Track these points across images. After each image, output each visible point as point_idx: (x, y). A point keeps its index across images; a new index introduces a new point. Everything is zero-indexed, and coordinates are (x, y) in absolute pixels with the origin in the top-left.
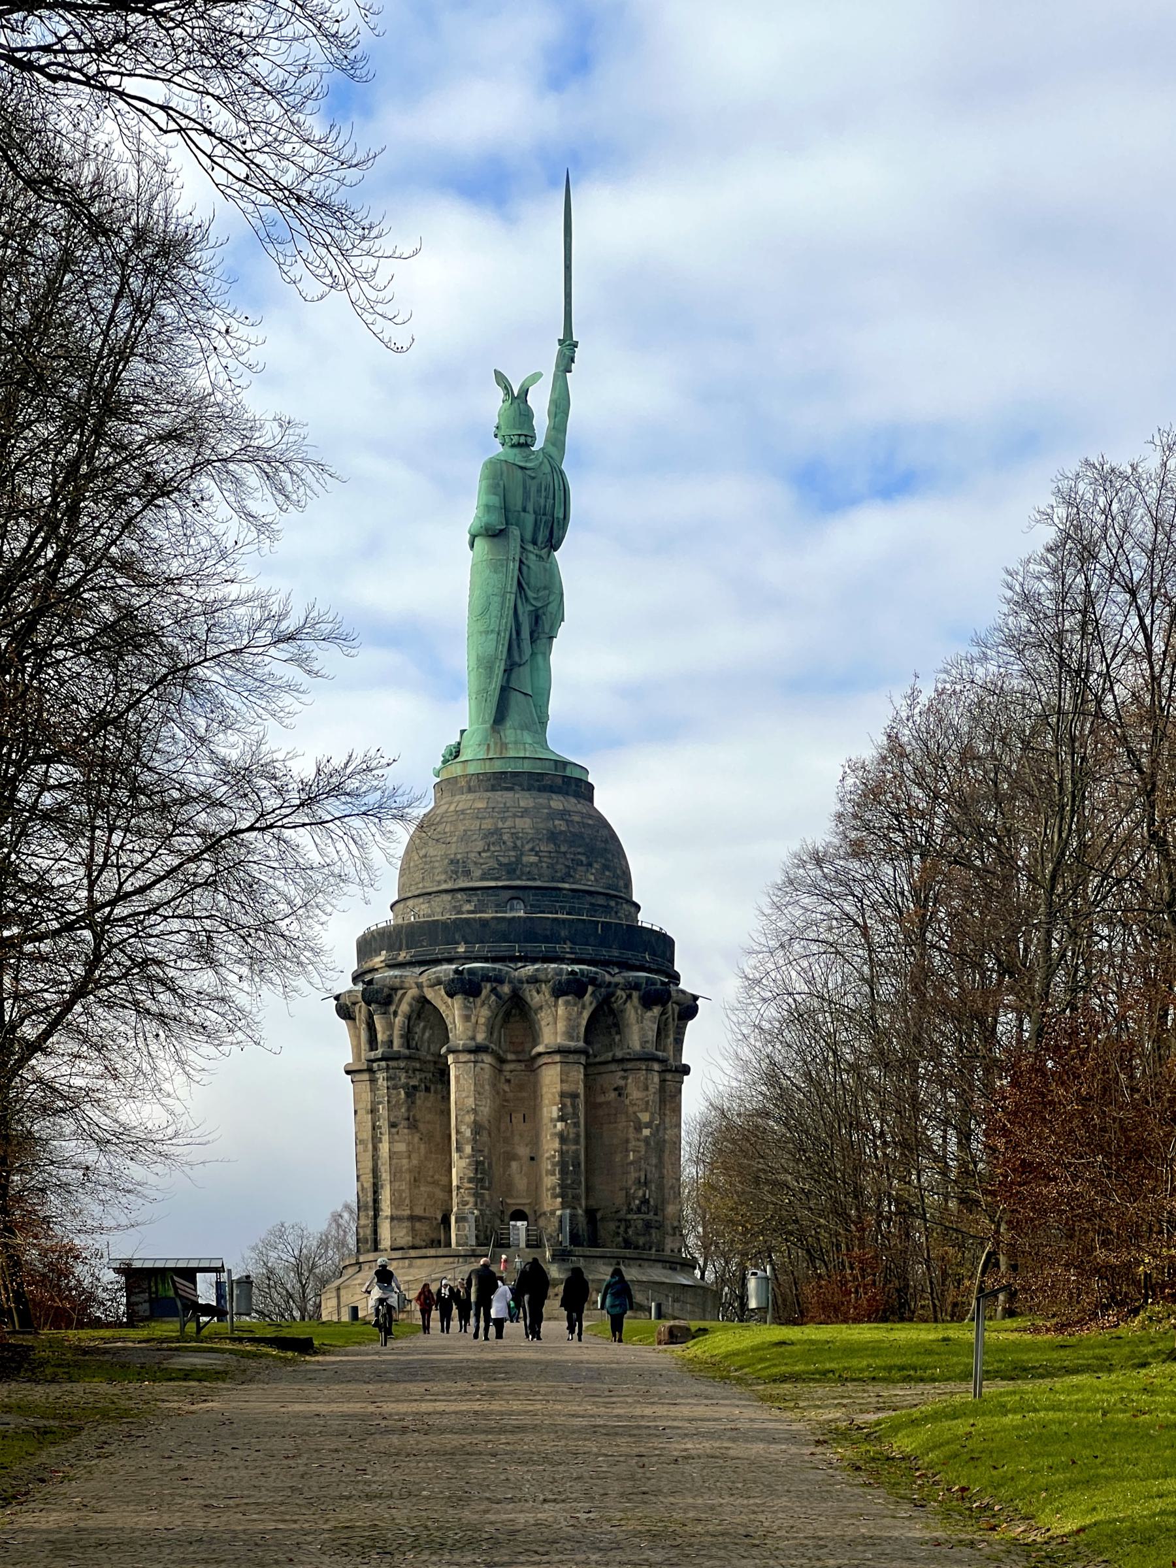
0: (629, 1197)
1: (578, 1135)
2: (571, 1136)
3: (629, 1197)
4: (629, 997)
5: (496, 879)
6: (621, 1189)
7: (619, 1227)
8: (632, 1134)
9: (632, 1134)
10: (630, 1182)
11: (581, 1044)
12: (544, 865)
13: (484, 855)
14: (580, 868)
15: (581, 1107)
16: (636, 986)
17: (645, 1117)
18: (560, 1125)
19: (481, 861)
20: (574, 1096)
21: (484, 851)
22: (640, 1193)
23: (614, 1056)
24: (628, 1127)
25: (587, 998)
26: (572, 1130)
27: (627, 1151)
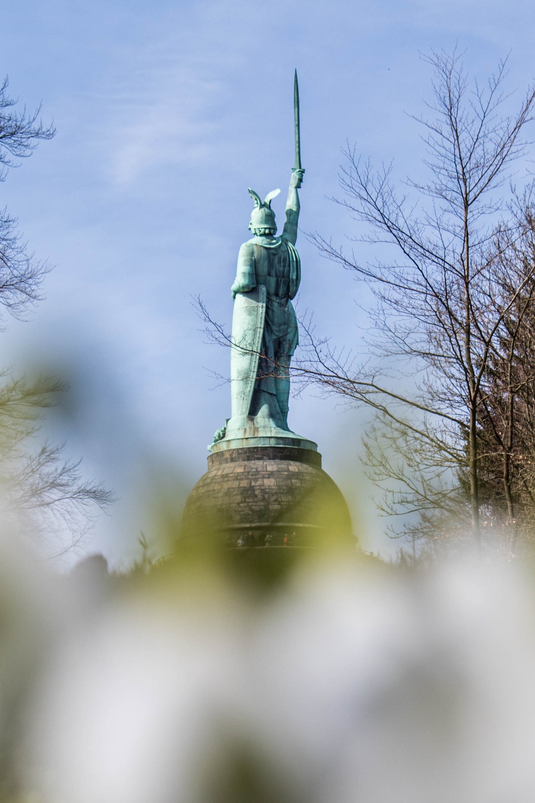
19: (240, 509)
21: (242, 502)
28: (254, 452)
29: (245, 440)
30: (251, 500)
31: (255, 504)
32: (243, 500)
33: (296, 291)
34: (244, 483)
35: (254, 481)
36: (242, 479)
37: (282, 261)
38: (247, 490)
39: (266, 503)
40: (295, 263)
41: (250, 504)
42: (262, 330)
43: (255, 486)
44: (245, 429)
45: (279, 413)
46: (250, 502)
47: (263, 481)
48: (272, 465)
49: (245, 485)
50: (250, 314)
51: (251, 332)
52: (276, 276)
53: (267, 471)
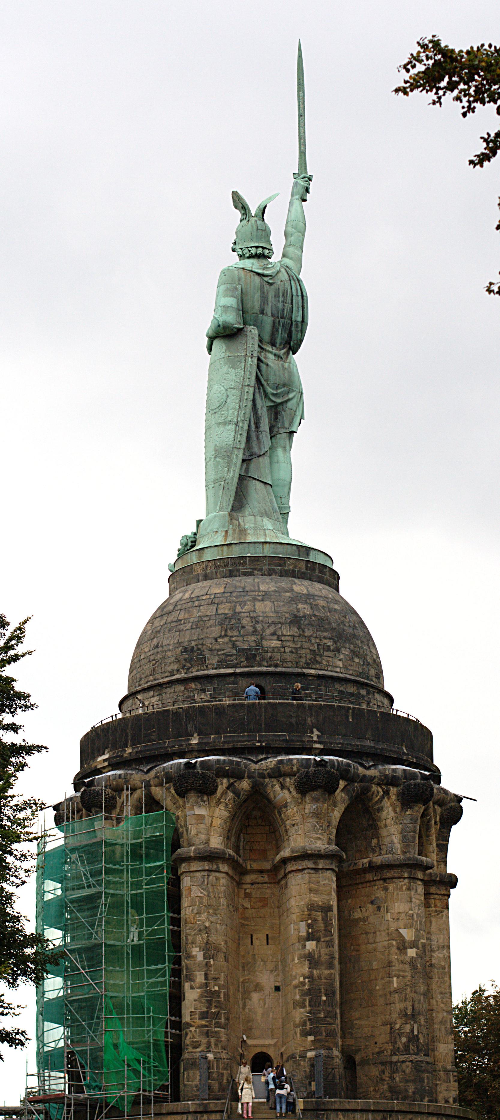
0: (394, 1035)
1: (332, 957)
2: (324, 958)
3: (394, 1035)
4: (386, 793)
5: (235, 666)
6: (384, 1024)
7: (383, 1072)
8: (394, 957)
9: (395, 956)
10: (395, 1016)
11: (334, 847)
12: (287, 650)
13: (220, 640)
14: (326, 653)
15: (335, 922)
16: (392, 781)
17: (408, 934)
18: (311, 945)
19: (218, 647)
20: (327, 909)
21: (221, 637)
22: (407, 1028)
23: (370, 863)
24: (390, 946)
25: (339, 794)
26: (324, 951)
27: (390, 976)
28: (240, 564)
29: (225, 548)
30: (236, 633)
31: (241, 639)
32: (223, 633)
33: (301, 341)
34: (225, 609)
35: (240, 605)
36: (222, 603)
37: (281, 294)
38: (230, 619)
39: (259, 637)
40: (300, 298)
41: (234, 639)
42: (251, 390)
43: (241, 612)
44: (226, 532)
45: (276, 512)
46: (233, 637)
47: (254, 605)
48: (267, 583)
49: (227, 611)
50: (233, 367)
51: (237, 392)
52: (273, 315)
53: (259, 591)
